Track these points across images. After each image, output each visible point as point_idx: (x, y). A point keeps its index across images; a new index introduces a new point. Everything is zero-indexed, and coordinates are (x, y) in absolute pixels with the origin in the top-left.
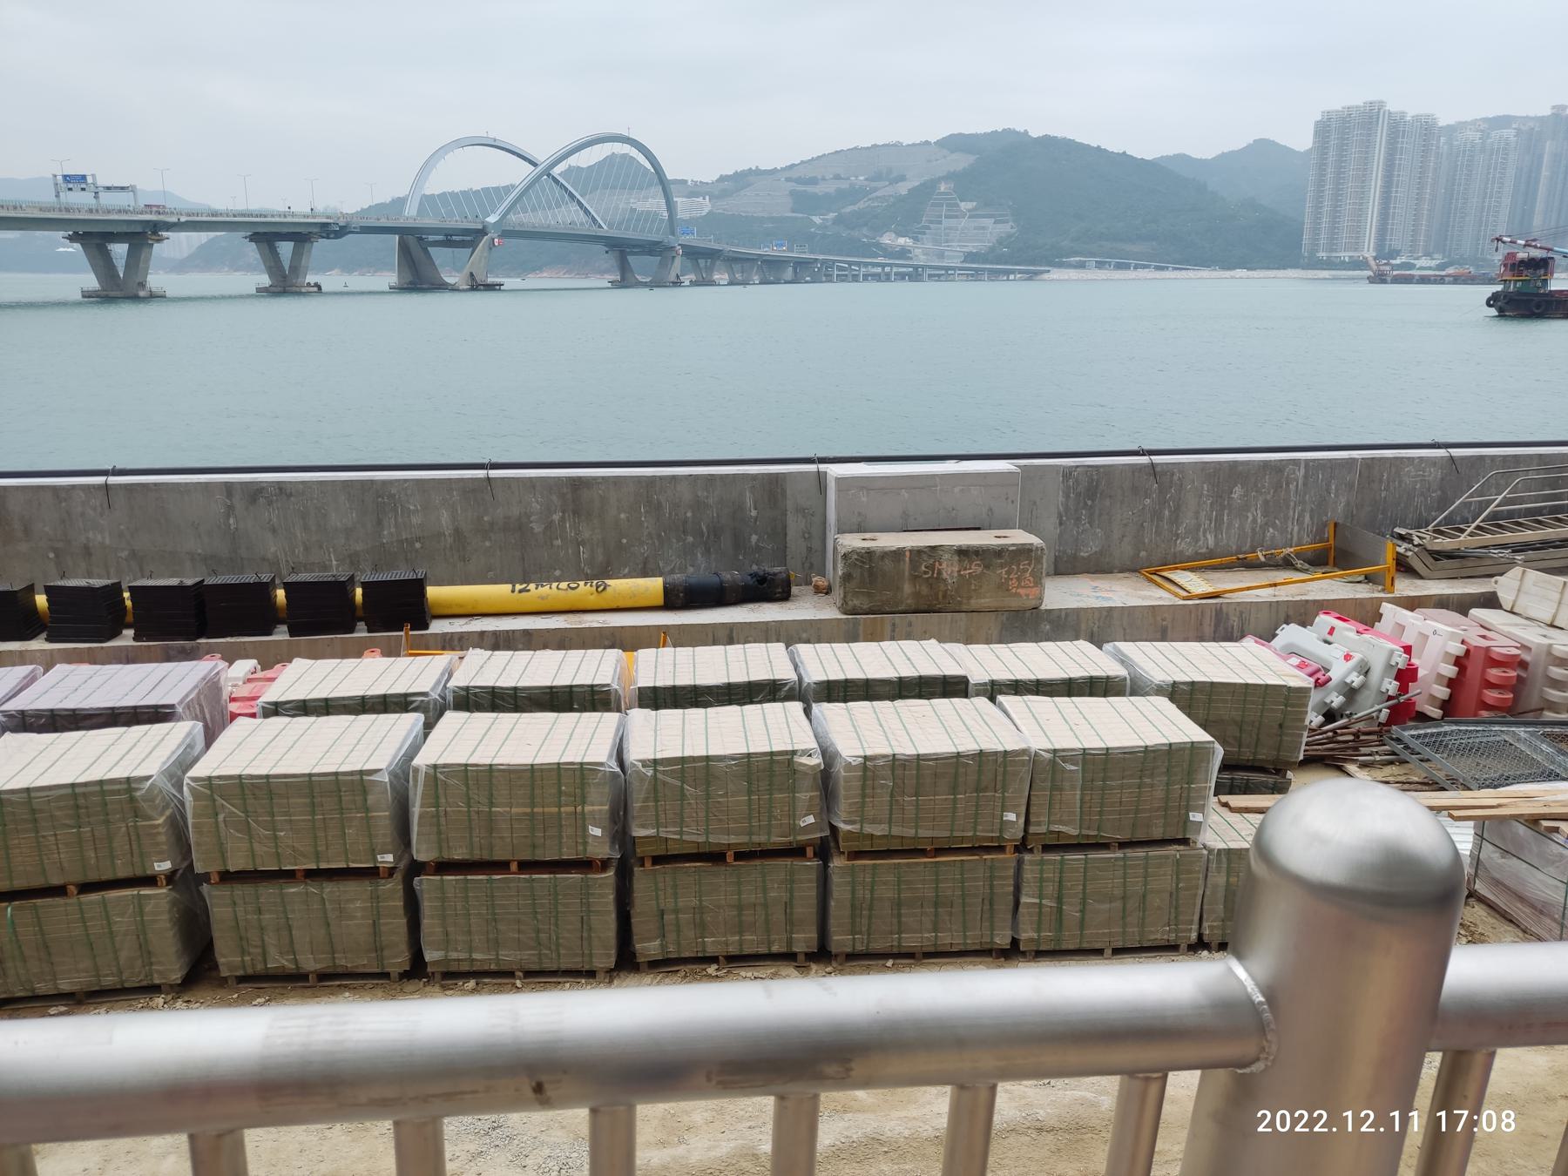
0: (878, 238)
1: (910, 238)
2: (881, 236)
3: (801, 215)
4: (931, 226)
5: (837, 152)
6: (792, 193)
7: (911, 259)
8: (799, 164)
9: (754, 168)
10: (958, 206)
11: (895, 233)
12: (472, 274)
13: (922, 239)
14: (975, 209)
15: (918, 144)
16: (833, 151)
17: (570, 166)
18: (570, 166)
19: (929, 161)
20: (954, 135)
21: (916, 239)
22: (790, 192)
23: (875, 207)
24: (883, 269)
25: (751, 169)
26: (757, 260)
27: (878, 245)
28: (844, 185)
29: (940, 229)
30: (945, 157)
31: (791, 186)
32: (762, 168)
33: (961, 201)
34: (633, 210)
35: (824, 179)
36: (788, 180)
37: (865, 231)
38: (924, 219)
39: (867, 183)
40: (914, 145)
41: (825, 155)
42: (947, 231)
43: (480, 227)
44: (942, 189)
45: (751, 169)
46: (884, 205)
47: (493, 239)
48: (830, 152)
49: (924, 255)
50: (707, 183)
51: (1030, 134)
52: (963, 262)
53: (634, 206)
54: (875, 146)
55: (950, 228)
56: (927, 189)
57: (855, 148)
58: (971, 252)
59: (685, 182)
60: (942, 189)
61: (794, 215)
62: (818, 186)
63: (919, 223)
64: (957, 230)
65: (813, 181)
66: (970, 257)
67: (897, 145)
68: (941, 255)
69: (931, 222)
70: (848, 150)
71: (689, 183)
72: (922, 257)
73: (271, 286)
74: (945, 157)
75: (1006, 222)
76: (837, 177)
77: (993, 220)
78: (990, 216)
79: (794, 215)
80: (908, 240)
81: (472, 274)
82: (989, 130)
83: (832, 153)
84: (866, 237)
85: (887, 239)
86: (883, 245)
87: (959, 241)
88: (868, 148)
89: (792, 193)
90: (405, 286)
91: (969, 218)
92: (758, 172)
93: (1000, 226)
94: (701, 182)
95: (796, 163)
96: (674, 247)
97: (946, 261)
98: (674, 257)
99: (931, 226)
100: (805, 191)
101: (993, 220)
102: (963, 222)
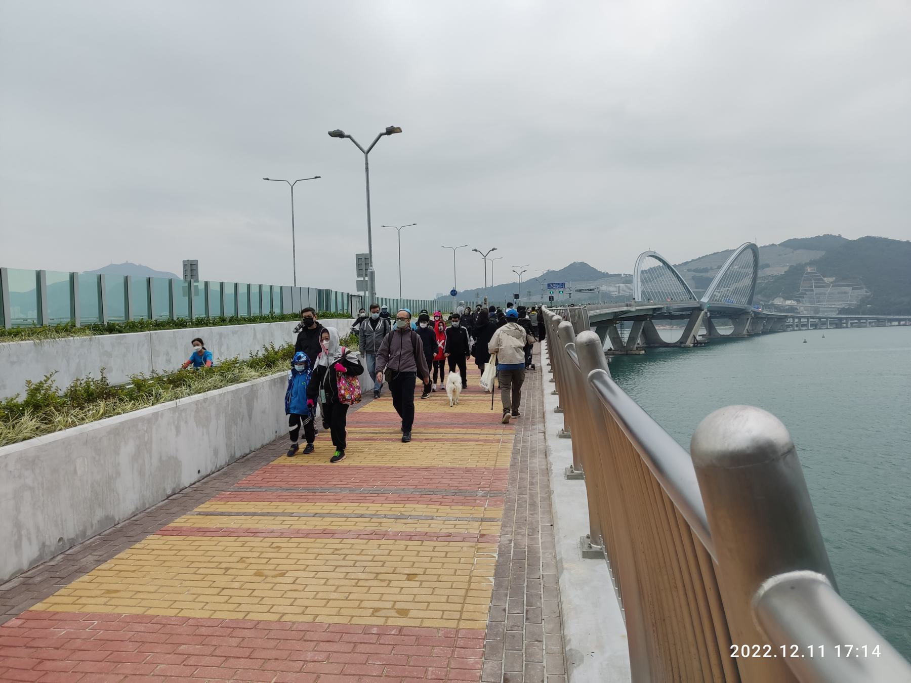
1: (794, 301)
4: (807, 293)
5: (715, 253)
6: (694, 278)
7: (799, 313)
8: (691, 261)
10: (823, 280)
11: (783, 298)
12: (694, 335)
13: (803, 301)
14: (834, 282)
15: (767, 246)
19: (780, 255)
20: (791, 240)
21: (798, 301)
24: (808, 320)
26: (765, 318)
27: (773, 305)
30: (793, 252)
31: (692, 274)
35: (711, 269)
36: (689, 270)
40: (764, 247)
43: (699, 306)
44: (809, 270)
47: (706, 313)
48: (710, 253)
49: (805, 310)
51: (842, 237)
52: (838, 314)
55: (820, 294)
56: (796, 272)
58: (844, 308)
59: (619, 275)
60: (809, 270)
62: (709, 273)
63: (798, 292)
68: (817, 311)
70: (722, 252)
71: (623, 275)
72: (805, 312)
73: (609, 350)
74: (793, 252)
77: (851, 288)
78: (848, 286)
80: (793, 302)
81: (694, 335)
82: (814, 236)
83: (712, 254)
90: (645, 345)
91: (832, 287)
94: (629, 275)
96: (748, 313)
97: (821, 314)
98: (748, 319)
99: (807, 293)
100: (702, 276)
101: (851, 288)
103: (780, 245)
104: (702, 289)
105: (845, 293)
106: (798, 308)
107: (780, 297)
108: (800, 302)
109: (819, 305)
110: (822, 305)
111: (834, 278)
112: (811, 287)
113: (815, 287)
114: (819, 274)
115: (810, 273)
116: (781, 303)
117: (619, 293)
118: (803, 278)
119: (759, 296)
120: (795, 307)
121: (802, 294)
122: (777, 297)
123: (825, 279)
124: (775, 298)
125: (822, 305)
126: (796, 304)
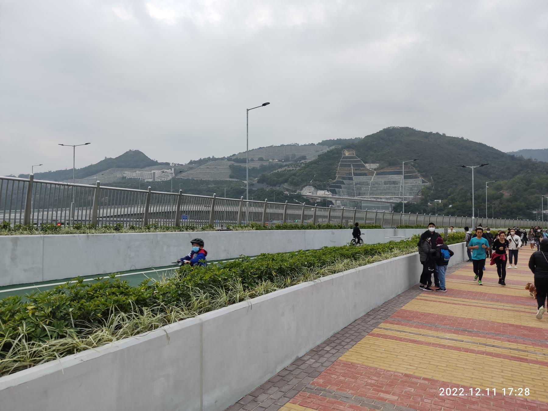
0: (298, 191)
1: (328, 191)
2: (301, 190)
3: (237, 180)
4: (344, 181)
5: (260, 148)
6: (231, 167)
9: (211, 157)
10: (364, 167)
13: (339, 192)
16: (259, 147)
17: (106, 157)
18: (106, 157)
21: (334, 192)
23: (290, 170)
25: (210, 158)
27: (300, 198)
28: (266, 164)
29: (352, 184)
32: (216, 157)
33: (366, 163)
34: (124, 178)
37: (286, 186)
38: (337, 176)
39: (279, 163)
40: (304, 145)
41: (253, 149)
42: (359, 186)
44: (347, 154)
45: (210, 158)
46: (297, 169)
50: (182, 165)
53: (125, 175)
54: (283, 145)
55: (361, 184)
57: (271, 146)
61: (231, 179)
64: (368, 184)
65: (244, 161)
66: (397, 208)
67: (295, 146)
69: (344, 178)
70: (267, 147)
74: (329, 148)
75: (416, 177)
76: (261, 159)
79: (231, 179)
80: (327, 193)
84: (287, 190)
85: (307, 192)
86: (305, 197)
87: (371, 194)
88: (279, 146)
89: (231, 167)
91: (377, 174)
92: (214, 159)
93: (411, 180)
94: (178, 164)
99: (344, 181)
101: (403, 176)
102: (373, 179)
103: (319, 144)
104: (237, 178)
105: (394, 183)
106: (334, 202)
107: (310, 185)
108: (337, 194)
109: (361, 198)
110: (365, 198)
111: (378, 165)
112: (350, 174)
113: (355, 174)
114: (359, 159)
115: (347, 157)
116: (310, 194)
117: (154, 179)
118: (340, 163)
119: (286, 184)
120: (329, 199)
121: (338, 182)
122: (306, 185)
123: (367, 165)
124: (304, 187)
125: (365, 198)
126: (330, 196)
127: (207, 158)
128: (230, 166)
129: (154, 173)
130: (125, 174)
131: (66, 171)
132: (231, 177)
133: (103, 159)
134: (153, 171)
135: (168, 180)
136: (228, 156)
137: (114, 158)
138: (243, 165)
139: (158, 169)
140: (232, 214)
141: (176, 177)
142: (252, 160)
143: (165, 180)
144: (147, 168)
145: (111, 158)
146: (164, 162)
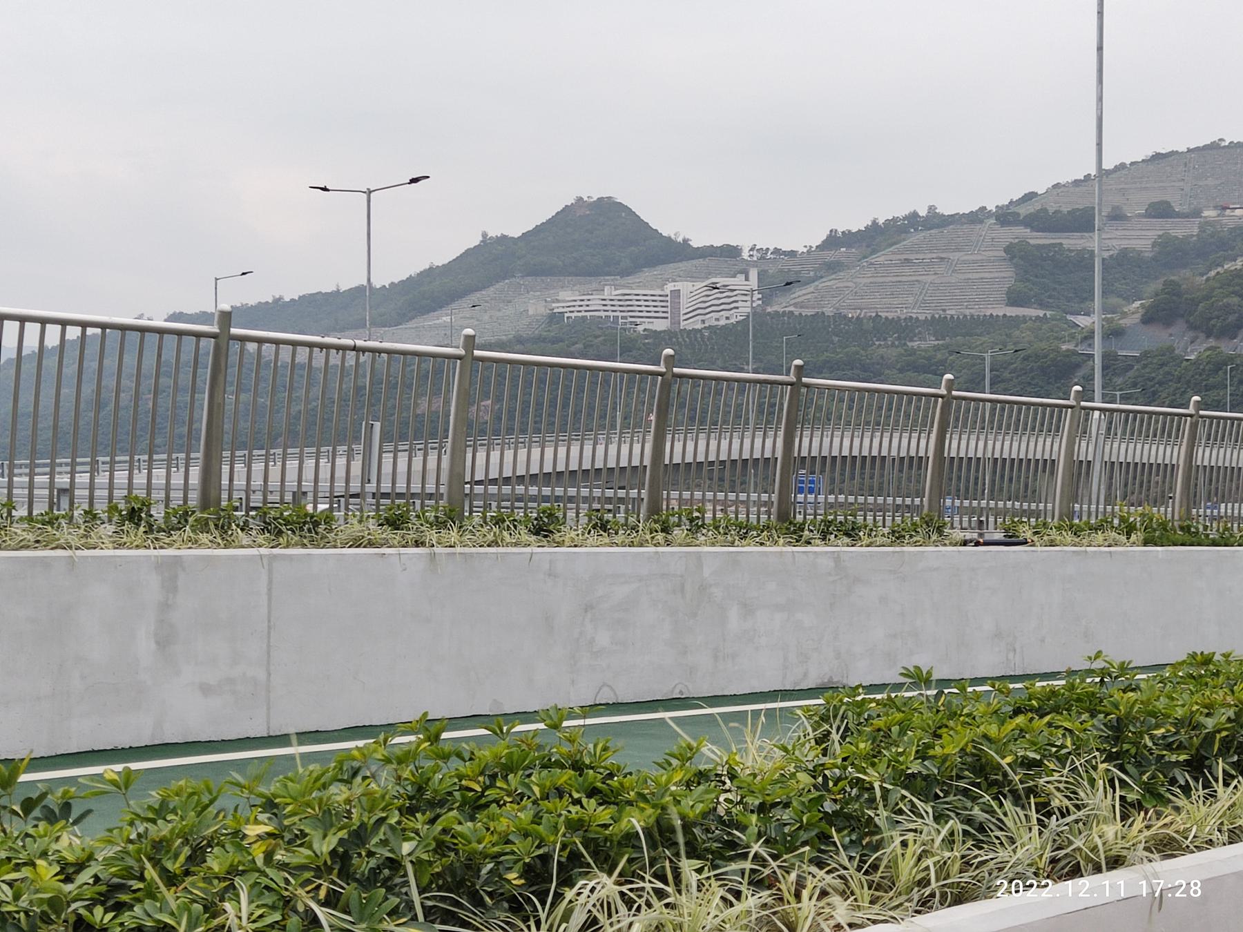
3: (1041, 313)
5: (1157, 157)
6: (1012, 251)
9: (923, 213)
16: (1150, 154)
17: (484, 235)
18: (484, 235)
22: (1008, 250)
32: (946, 209)
34: (555, 318)
35: (1117, 216)
45: (915, 215)
50: (792, 253)
53: (558, 308)
65: (1082, 222)
71: (745, 255)
76: (1161, 211)
89: (1012, 251)
92: (935, 221)
94: (777, 251)
95: (1040, 192)
104: (1042, 305)
127: (904, 219)
128: (1008, 250)
129: (676, 294)
130: (558, 301)
131: (337, 293)
132: (1014, 299)
133: (476, 241)
134: (670, 287)
135: (733, 320)
136: (1000, 204)
137: (516, 233)
138: (1072, 242)
139: (691, 277)
140: (969, 470)
141: (769, 310)
142: (1117, 216)
143: (723, 322)
144: (647, 274)
145: (504, 237)
146: (717, 244)
